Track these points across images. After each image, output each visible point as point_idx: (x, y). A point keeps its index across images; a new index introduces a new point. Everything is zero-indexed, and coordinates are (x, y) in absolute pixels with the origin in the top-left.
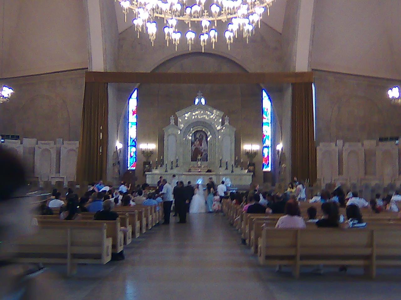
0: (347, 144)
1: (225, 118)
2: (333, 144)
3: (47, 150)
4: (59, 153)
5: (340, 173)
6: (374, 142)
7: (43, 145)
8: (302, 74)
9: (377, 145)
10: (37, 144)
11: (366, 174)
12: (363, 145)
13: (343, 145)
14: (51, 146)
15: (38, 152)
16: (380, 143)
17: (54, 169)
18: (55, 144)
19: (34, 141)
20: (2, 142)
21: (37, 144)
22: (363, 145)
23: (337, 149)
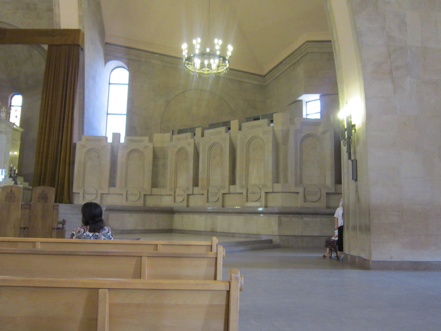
1: (2, 110)
5: (112, 184)
6: (167, 136)
11: (155, 184)
12: (151, 140)
22: (151, 140)
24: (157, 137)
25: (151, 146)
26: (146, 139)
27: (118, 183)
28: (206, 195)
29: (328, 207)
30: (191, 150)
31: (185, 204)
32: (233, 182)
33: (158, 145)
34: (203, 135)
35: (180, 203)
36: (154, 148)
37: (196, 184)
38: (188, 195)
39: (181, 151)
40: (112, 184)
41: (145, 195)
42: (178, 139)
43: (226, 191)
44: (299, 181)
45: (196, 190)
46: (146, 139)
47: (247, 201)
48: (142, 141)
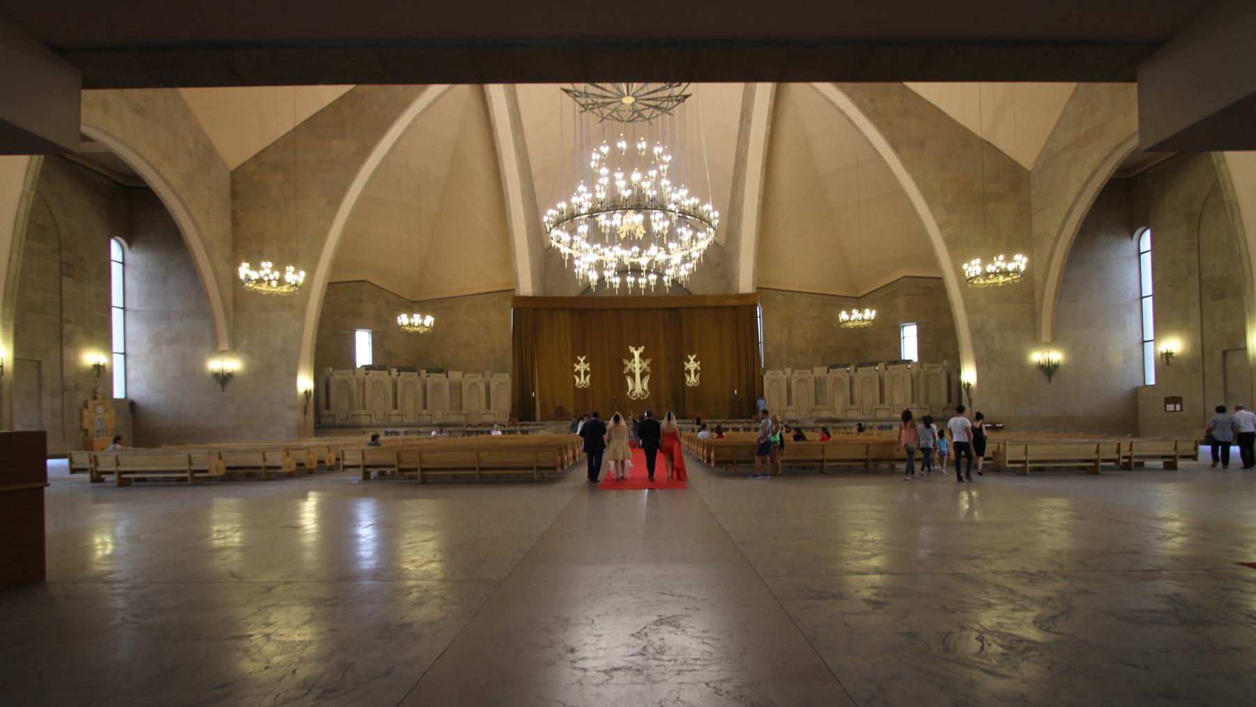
0: (796, 372)
2: (781, 372)
3: (474, 384)
4: (488, 388)
5: (789, 403)
7: (471, 378)
8: (746, 296)
9: (828, 372)
10: (463, 376)
11: (816, 403)
13: (792, 373)
14: (478, 379)
15: (465, 387)
16: (831, 370)
17: (484, 405)
18: (483, 376)
19: (461, 373)
20: (427, 376)
21: (463, 376)
22: (813, 373)
23: (785, 377)
24: (816, 369)
25: (813, 376)
26: (809, 371)
27: (793, 403)
28: (861, 408)
29: (944, 416)
30: (846, 380)
31: (845, 416)
32: (882, 401)
33: (818, 376)
34: (856, 371)
35: (839, 414)
36: (815, 378)
37: (852, 402)
38: (847, 410)
39: (837, 381)
40: (789, 403)
41: (812, 411)
42: (835, 372)
43: (878, 407)
44: (927, 401)
45: (853, 407)
46: (809, 371)
47: (894, 413)
48: (806, 373)
